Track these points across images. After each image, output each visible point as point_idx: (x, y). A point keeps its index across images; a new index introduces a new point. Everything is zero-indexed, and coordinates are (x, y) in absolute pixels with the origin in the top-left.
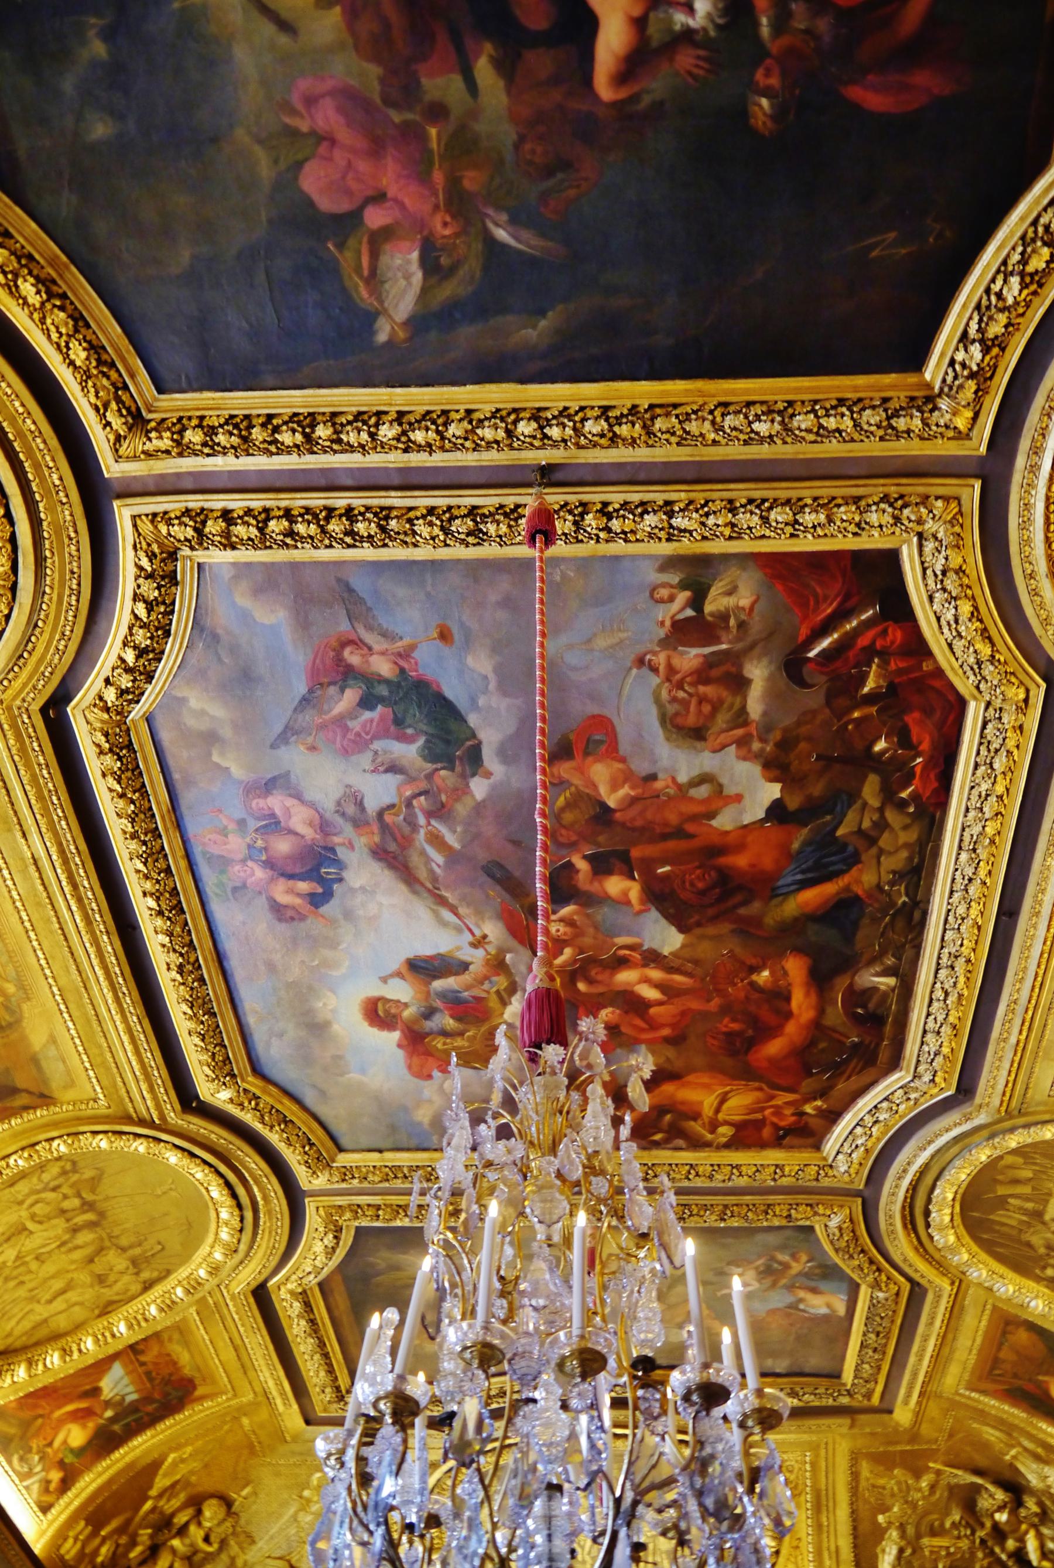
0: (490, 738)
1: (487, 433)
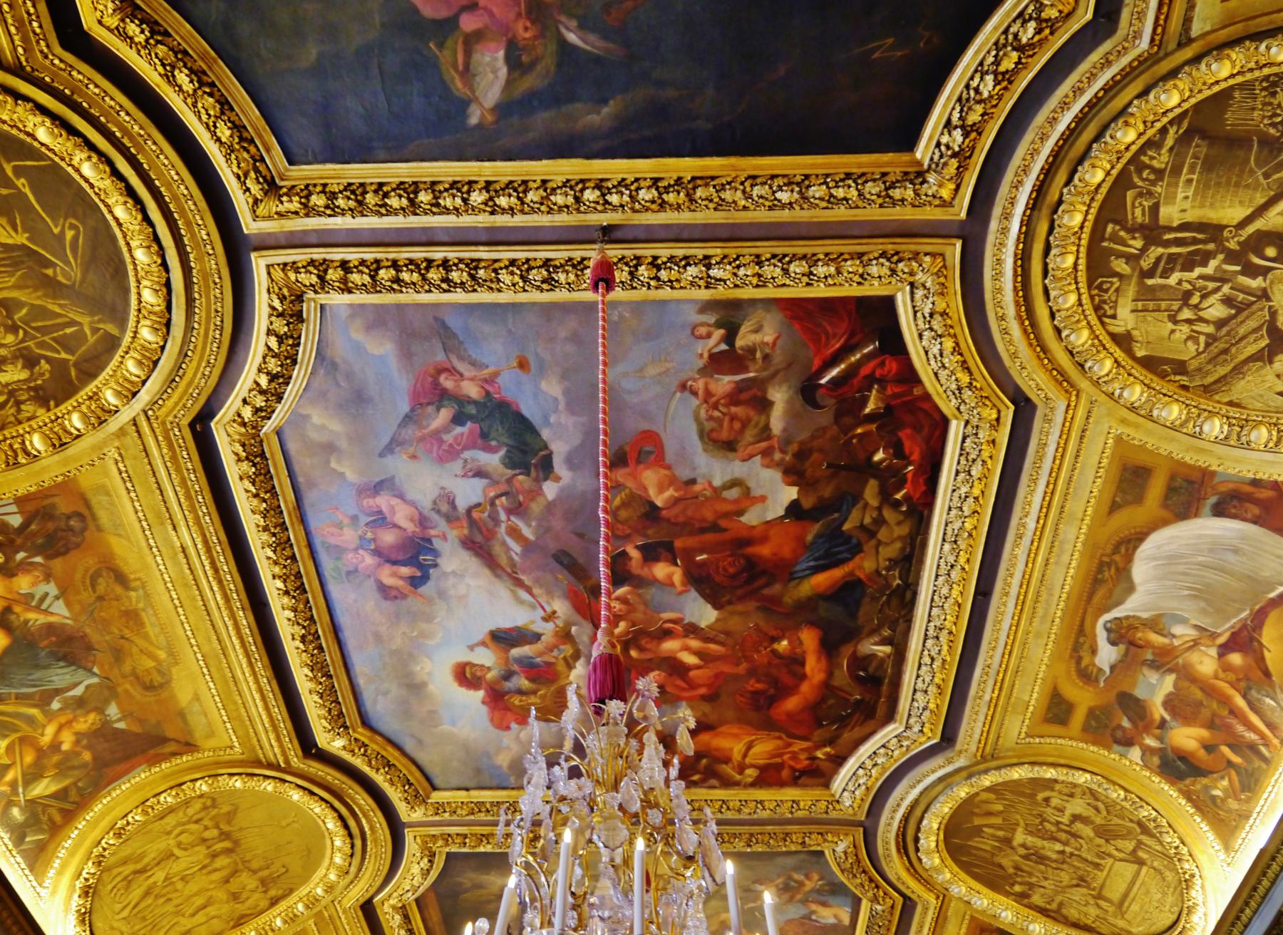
0: (559, 450)
1: (559, 199)
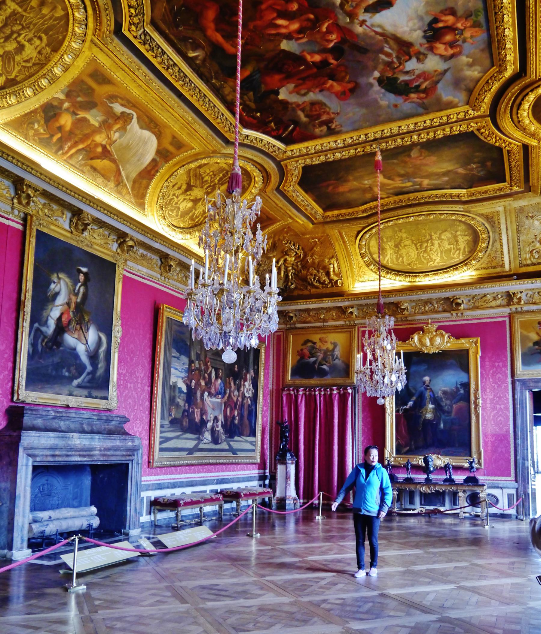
0: (377, 87)
